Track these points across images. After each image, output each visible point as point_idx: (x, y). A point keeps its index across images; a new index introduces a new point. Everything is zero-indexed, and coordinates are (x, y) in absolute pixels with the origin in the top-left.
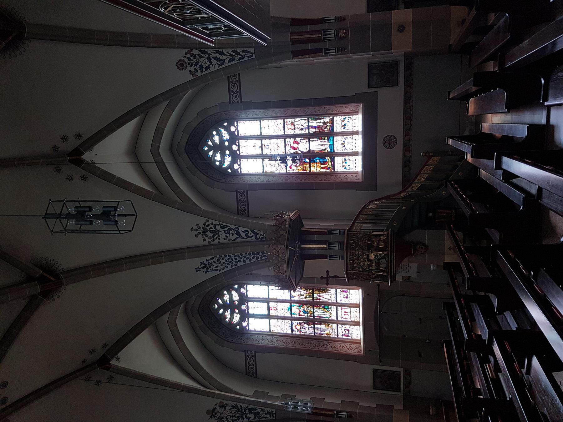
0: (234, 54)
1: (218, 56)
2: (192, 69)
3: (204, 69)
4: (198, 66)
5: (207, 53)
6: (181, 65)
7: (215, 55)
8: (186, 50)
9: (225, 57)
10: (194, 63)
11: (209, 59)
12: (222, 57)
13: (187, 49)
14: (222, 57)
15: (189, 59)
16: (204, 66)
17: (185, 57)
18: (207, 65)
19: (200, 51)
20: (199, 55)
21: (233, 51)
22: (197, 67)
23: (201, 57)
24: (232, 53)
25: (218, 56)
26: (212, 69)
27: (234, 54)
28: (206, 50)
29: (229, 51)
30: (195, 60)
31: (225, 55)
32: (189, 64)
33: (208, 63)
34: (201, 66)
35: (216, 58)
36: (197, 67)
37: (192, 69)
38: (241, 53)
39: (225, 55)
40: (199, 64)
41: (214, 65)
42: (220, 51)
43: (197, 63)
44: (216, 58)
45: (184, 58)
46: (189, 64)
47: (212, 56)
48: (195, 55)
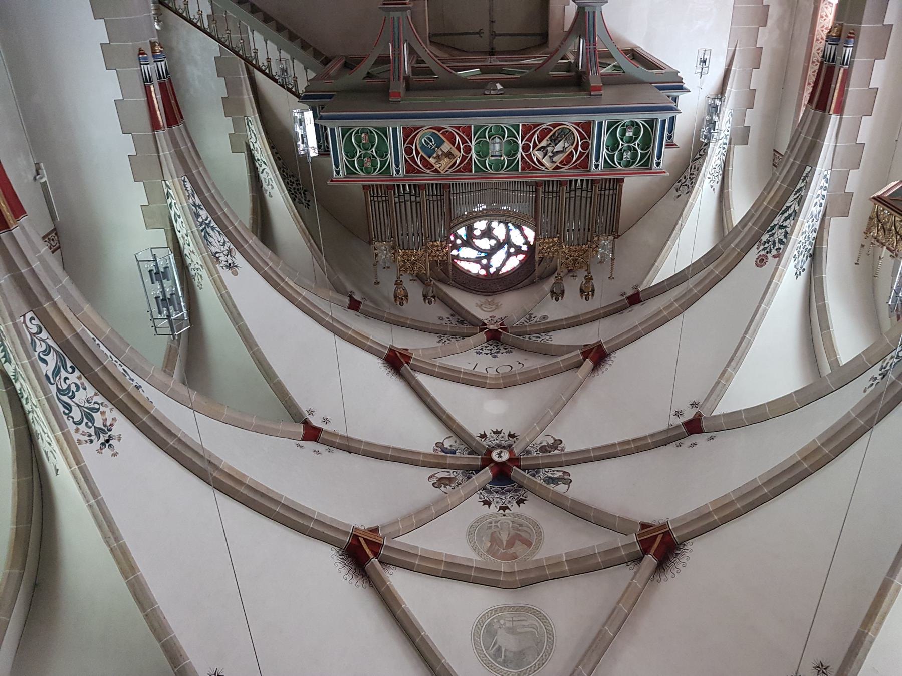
0: (798, 195)
1: (786, 215)
2: (774, 252)
3: (784, 240)
4: (777, 245)
5: (775, 225)
6: (761, 262)
7: (783, 218)
8: (756, 246)
9: (793, 207)
10: (772, 247)
11: (781, 227)
12: (790, 212)
13: (757, 244)
14: (790, 212)
15: (764, 249)
16: (782, 237)
17: (759, 252)
18: (783, 234)
19: (768, 232)
20: (769, 237)
21: (795, 194)
22: (778, 245)
23: (772, 235)
24: (795, 197)
25: (786, 215)
26: (788, 230)
27: (798, 195)
28: (772, 225)
29: (791, 198)
30: (770, 243)
31: (791, 206)
32: (767, 253)
33: (783, 230)
34: (781, 242)
35: (786, 219)
36: (778, 245)
37: (774, 252)
38: (803, 185)
39: (791, 206)
40: (777, 241)
41: (789, 226)
42: (785, 209)
43: (774, 244)
44: (786, 219)
45: (759, 254)
46: (767, 253)
47: (782, 221)
48: (767, 240)
